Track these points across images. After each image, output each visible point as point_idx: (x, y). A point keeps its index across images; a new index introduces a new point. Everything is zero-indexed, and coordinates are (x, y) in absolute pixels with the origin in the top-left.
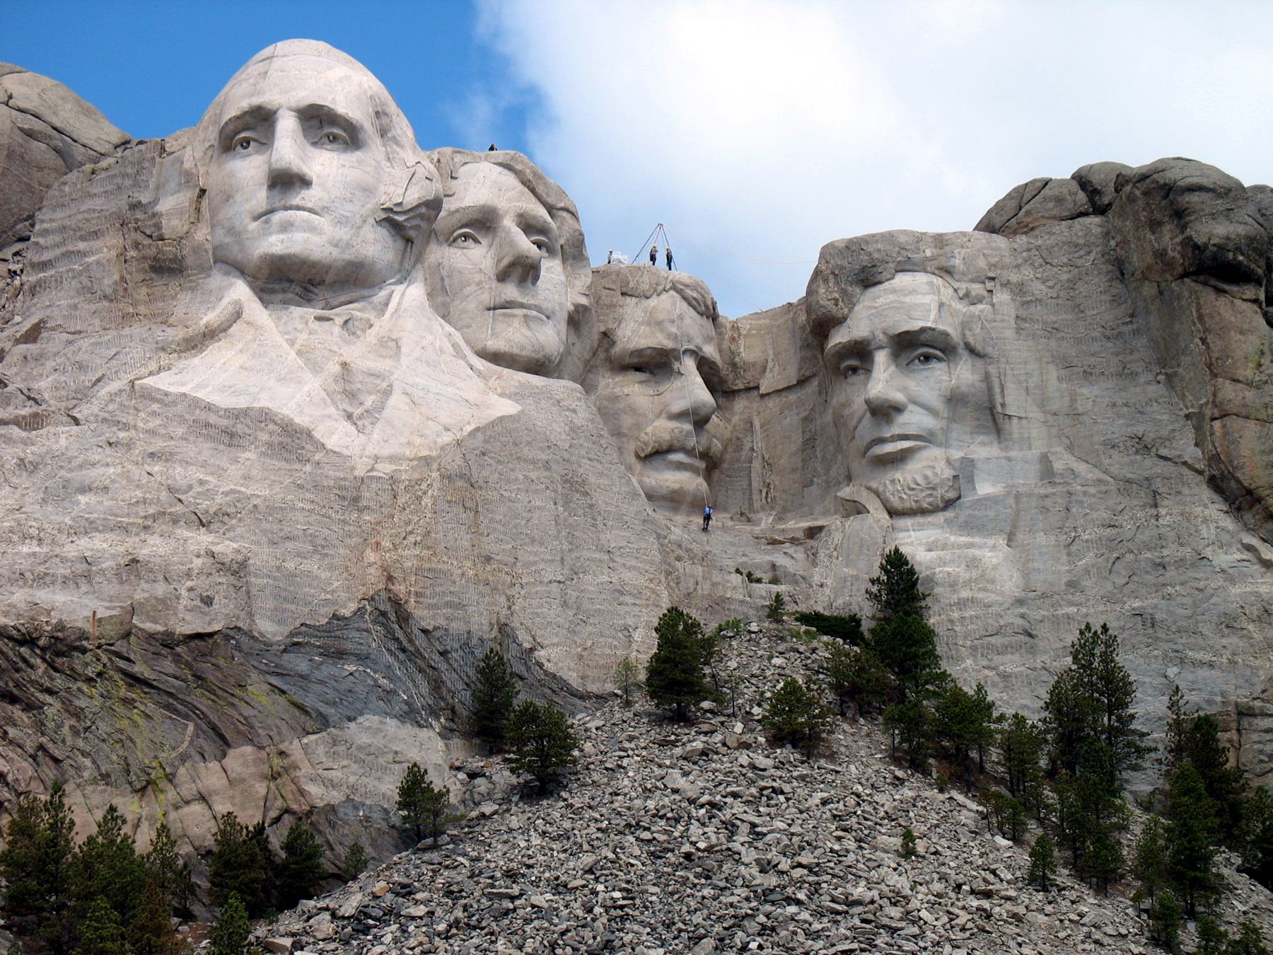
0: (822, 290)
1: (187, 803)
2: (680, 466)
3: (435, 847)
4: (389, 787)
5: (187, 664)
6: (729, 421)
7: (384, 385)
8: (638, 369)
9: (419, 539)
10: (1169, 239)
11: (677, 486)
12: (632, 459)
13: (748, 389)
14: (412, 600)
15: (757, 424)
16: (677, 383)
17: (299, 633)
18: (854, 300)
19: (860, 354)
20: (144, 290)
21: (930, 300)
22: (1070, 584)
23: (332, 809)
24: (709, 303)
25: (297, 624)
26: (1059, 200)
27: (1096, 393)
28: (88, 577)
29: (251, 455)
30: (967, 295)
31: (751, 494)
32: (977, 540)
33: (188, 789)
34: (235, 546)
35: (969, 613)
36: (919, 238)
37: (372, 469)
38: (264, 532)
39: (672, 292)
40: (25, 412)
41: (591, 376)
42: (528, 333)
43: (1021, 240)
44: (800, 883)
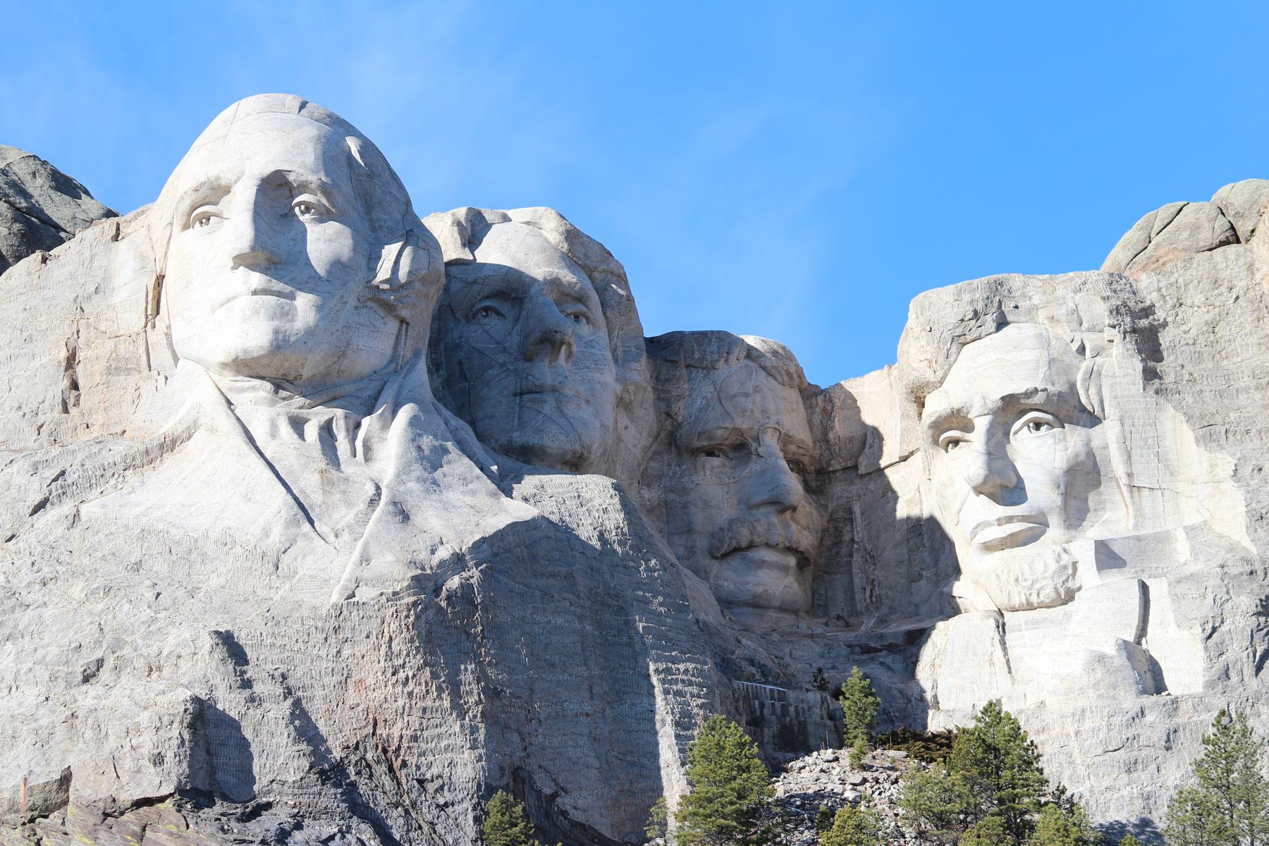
0: (913, 351)
2: (762, 564)
5: (134, 834)
6: (826, 507)
7: (371, 490)
8: (710, 453)
9: (410, 674)
11: (760, 589)
12: (706, 562)
13: (844, 469)
14: (406, 745)
15: (857, 510)
16: (755, 466)
17: (269, 792)
18: (952, 359)
22: (1210, 685)
24: (792, 369)
25: (265, 782)
26: (1195, 228)
27: (1239, 455)
30: (1082, 350)
31: (853, 593)
34: (189, 693)
35: (1088, 725)
37: (353, 595)
38: (228, 674)
39: (749, 362)
41: (654, 464)
42: (563, 421)
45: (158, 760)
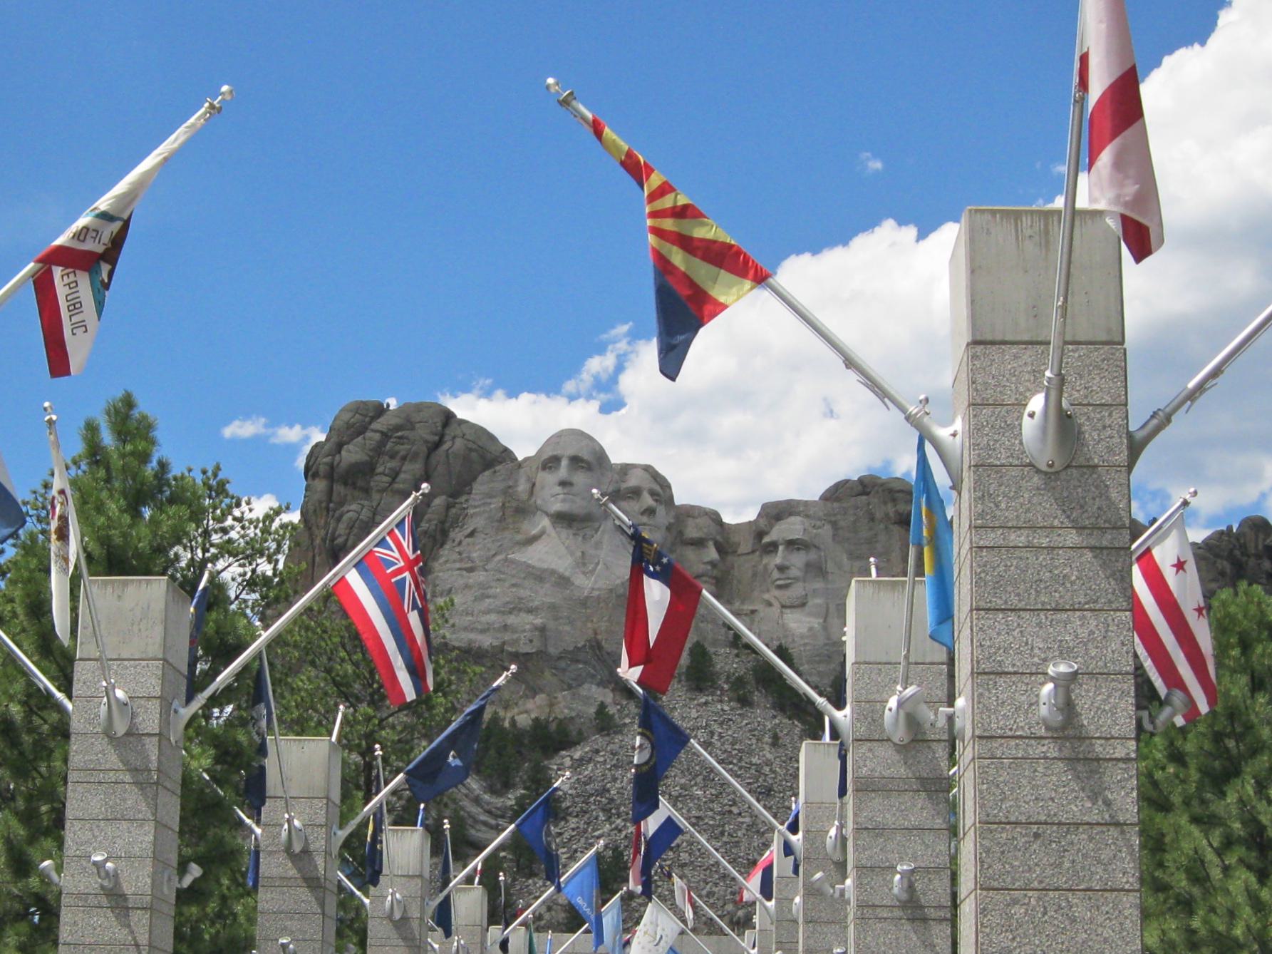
1: (521, 713)
3: (608, 735)
4: (592, 710)
10: (891, 509)
19: (772, 547)
20: (510, 520)
21: (799, 527)
23: (572, 718)
26: (852, 488)
28: (488, 629)
29: (547, 585)
32: (812, 619)
33: (522, 708)
36: (799, 502)
40: (469, 565)
43: (836, 505)
44: (734, 757)
45: (531, 641)
